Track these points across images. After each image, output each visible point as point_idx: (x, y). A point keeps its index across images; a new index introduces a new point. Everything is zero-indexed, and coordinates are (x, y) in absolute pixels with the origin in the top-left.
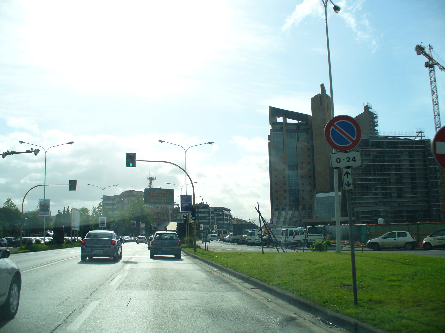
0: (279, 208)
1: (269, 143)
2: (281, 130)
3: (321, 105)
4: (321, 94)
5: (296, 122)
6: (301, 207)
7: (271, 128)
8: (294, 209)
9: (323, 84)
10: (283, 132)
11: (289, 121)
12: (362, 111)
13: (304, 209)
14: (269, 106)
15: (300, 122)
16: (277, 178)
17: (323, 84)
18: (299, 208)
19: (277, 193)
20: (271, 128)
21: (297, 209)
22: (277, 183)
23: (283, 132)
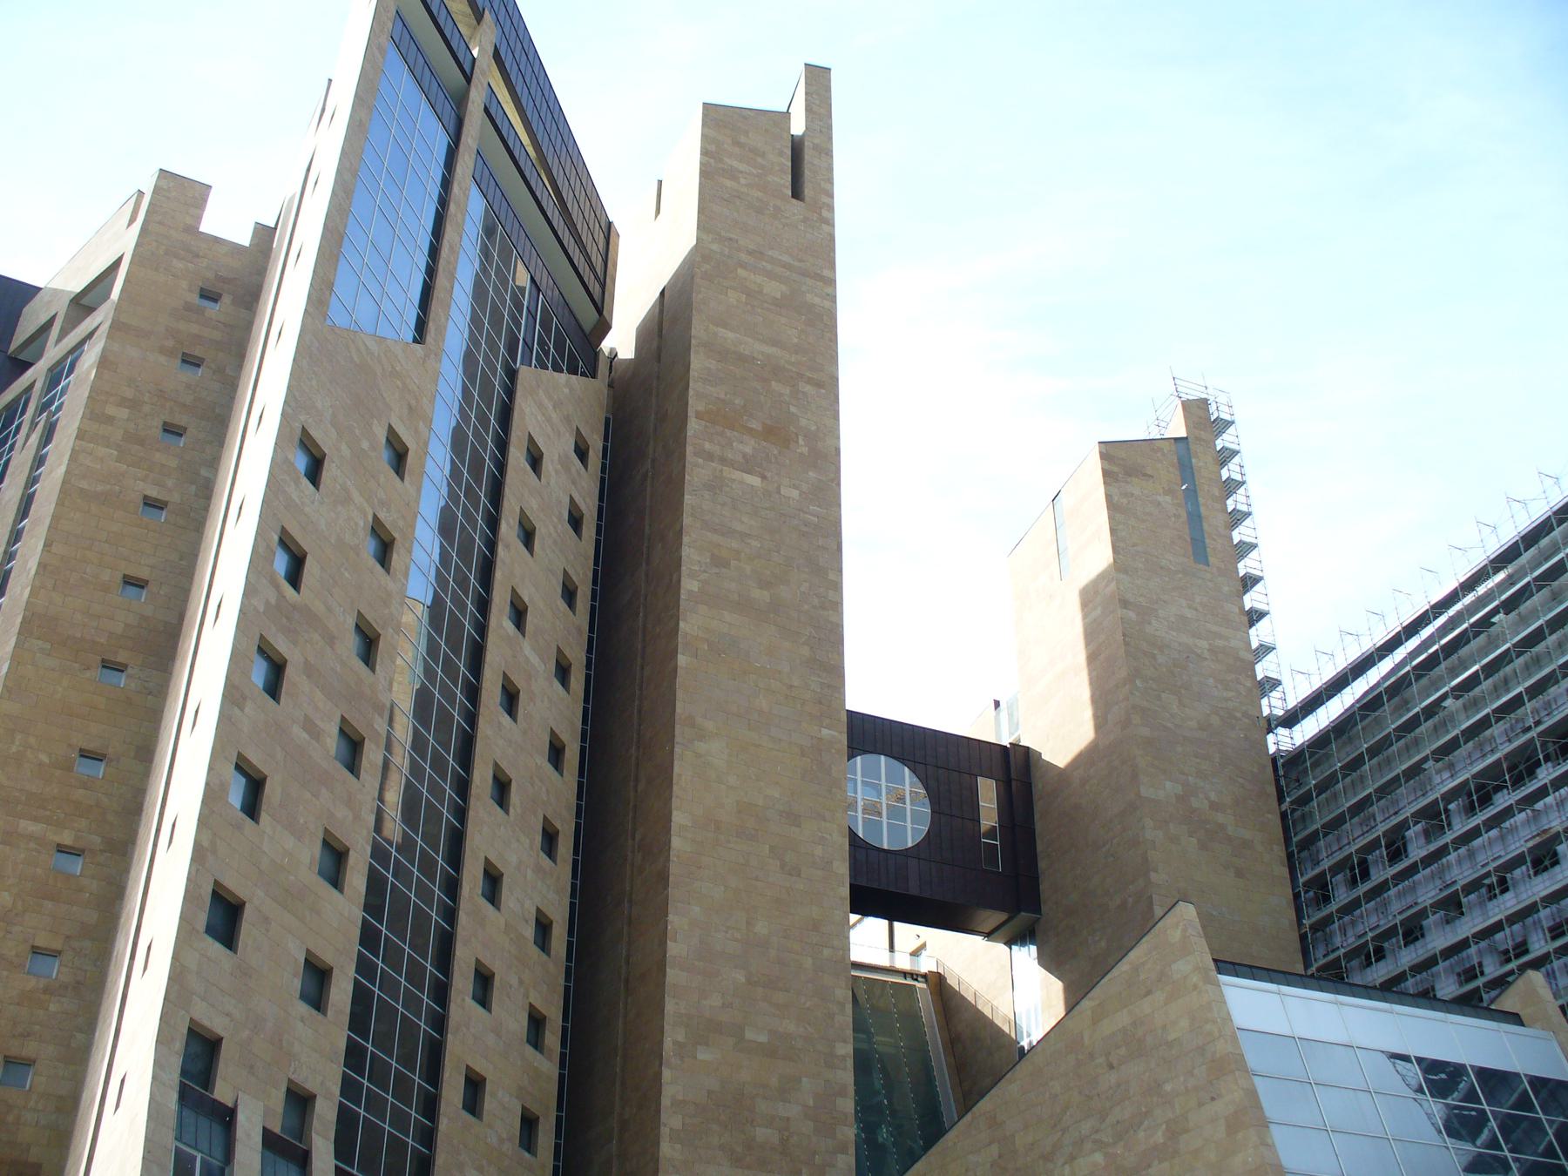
3: (797, 193)
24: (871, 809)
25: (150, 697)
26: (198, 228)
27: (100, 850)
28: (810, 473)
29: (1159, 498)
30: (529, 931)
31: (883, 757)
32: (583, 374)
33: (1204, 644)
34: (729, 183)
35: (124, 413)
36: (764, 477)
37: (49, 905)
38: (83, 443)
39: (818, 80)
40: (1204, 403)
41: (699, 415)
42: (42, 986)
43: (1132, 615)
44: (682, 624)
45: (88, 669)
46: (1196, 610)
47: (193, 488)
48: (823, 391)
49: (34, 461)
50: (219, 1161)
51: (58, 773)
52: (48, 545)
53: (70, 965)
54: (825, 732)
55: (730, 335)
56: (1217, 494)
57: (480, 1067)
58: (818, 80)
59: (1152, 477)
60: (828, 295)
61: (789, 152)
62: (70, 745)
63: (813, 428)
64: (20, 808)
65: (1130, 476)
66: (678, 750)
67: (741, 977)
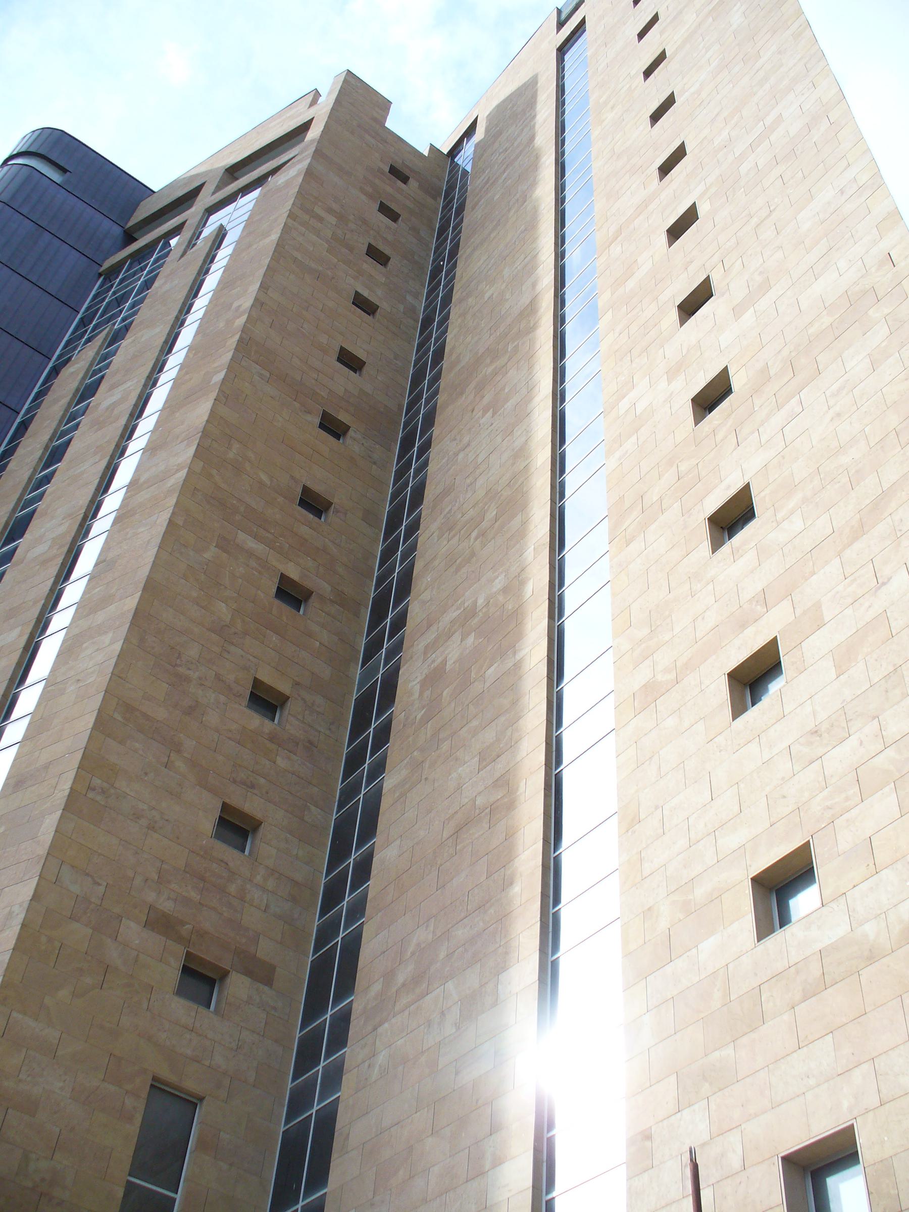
25: (374, 466)
26: (385, 124)
27: (330, 600)
35: (333, 220)
37: (274, 638)
38: (295, 223)
42: (267, 731)
45: (309, 413)
47: (401, 308)
49: (74, 395)
51: (280, 499)
52: (263, 287)
53: (300, 717)
62: (292, 477)
64: (238, 517)
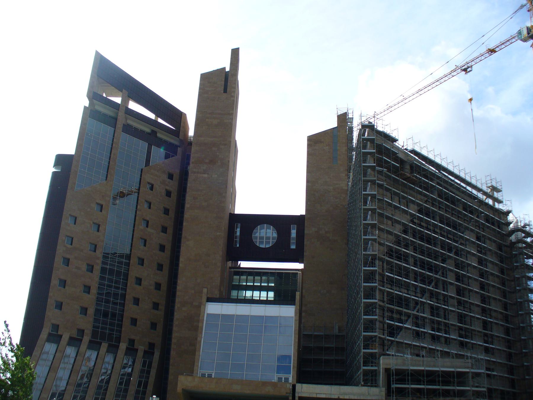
0: (61, 336)
1: (54, 173)
2: (112, 121)
3: (225, 91)
4: (228, 69)
5: (152, 116)
6: (123, 346)
7: (87, 105)
8: (104, 346)
9: (239, 48)
10: (115, 126)
11: (133, 106)
12: (333, 123)
13: (131, 351)
14: (96, 50)
15: (160, 120)
16: (71, 244)
17: (239, 48)
18: (117, 347)
19: (64, 287)
20: (87, 105)
21: (113, 348)
22: (69, 260)
23: (115, 126)
24: (261, 238)
28: (221, 170)
29: (325, 148)
30: (152, 288)
31: (265, 225)
32: (173, 156)
33: (331, 188)
34: (206, 95)
36: (208, 174)
39: (235, 53)
40: (345, 114)
41: (193, 163)
43: (310, 184)
44: (185, 216)
46: (331, 178)
48: (226, 146)
50: (51, 345)
54: (218, 233)
55: (202, 139)
56: (344, 141)
57: (134, 317)
58: (235, 53)
59: (323, 142)
60: (231, 118)
61: (224, 80)
63: (222, 157)
65: (316, 144)
66: (182, 245)
67: (193, 292)
